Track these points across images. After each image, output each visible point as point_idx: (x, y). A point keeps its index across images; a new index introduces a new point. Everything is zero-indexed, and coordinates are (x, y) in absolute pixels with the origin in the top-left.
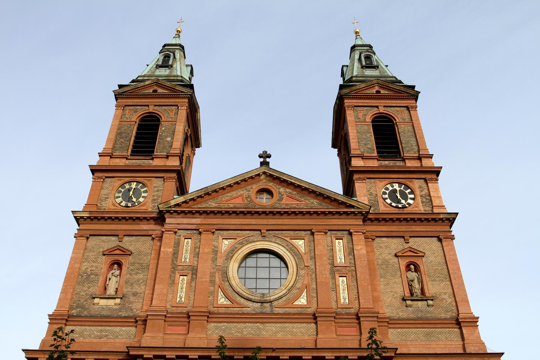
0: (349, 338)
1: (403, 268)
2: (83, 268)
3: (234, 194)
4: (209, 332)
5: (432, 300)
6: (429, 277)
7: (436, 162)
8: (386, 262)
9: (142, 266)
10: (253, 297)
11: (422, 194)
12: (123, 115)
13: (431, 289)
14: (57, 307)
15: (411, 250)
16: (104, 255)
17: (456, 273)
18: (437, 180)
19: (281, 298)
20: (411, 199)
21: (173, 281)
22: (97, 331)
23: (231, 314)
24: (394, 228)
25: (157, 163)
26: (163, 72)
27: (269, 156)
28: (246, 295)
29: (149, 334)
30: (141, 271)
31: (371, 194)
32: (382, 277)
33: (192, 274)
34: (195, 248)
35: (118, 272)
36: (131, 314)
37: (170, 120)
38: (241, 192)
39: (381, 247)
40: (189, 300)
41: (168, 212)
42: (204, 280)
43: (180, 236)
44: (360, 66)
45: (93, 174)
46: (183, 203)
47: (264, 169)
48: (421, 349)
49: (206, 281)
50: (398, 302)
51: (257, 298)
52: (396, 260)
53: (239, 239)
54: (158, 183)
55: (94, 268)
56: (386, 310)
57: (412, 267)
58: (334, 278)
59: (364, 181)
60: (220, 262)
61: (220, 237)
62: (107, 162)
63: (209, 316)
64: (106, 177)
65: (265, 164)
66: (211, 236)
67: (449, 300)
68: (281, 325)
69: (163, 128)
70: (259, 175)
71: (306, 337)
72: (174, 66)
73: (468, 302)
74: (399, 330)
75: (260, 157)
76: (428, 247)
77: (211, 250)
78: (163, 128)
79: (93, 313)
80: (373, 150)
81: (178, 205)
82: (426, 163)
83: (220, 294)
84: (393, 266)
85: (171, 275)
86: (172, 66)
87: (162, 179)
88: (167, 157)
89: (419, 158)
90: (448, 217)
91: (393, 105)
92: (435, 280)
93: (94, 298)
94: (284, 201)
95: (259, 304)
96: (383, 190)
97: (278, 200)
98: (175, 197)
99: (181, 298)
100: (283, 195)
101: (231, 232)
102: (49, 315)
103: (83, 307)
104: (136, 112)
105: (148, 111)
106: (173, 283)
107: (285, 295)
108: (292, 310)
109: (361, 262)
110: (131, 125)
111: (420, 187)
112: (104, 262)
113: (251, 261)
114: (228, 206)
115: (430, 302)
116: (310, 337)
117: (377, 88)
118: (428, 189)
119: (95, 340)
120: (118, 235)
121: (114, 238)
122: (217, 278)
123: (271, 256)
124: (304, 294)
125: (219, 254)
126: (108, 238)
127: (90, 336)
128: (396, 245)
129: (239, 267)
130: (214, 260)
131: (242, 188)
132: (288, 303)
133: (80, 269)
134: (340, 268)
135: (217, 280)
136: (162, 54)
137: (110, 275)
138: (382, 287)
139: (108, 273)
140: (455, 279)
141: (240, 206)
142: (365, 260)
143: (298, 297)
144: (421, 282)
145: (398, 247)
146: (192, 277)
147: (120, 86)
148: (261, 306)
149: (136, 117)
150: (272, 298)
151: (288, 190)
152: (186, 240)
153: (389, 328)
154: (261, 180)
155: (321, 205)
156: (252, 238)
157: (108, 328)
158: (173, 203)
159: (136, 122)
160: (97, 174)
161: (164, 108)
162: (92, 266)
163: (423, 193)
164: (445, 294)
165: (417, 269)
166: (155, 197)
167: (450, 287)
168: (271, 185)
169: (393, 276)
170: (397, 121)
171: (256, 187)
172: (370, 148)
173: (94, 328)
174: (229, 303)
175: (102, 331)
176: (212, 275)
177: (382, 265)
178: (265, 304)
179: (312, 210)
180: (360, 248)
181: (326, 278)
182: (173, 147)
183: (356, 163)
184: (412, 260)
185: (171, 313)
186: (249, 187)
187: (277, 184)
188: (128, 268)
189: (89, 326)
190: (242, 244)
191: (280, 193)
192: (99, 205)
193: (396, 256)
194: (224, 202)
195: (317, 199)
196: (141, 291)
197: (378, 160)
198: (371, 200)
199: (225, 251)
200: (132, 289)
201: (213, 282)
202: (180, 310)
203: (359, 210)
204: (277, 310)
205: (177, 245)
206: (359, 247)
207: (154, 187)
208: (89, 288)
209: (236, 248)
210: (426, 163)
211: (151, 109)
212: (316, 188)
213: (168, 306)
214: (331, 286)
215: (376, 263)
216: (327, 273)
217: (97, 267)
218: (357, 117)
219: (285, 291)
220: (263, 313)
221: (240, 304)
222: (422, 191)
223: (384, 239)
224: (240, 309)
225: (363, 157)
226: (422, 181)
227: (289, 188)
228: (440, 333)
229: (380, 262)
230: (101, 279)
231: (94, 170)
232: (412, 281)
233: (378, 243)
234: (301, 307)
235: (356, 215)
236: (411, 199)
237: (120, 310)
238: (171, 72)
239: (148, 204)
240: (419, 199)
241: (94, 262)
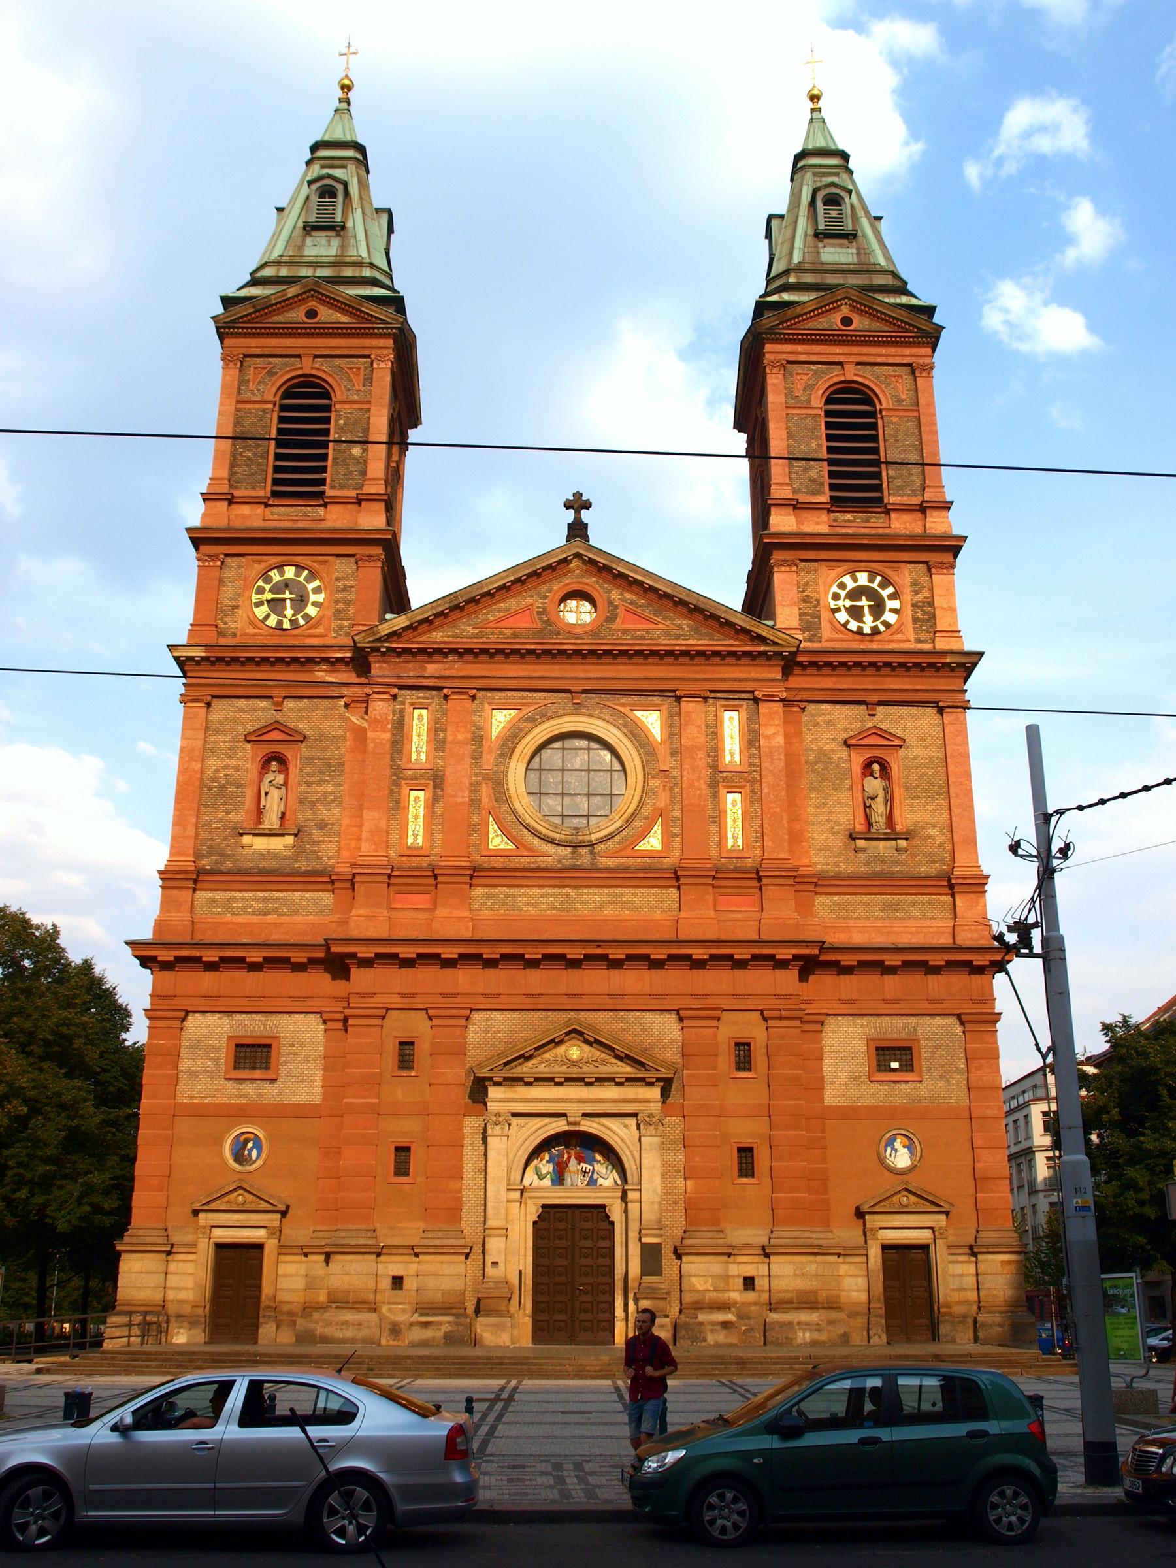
0: (739, 916)
1: (857, 769)
2: (210, 771)
3: (512, 604)
4: (475, 906)
5: (907, 839)
6: (908, 789)
7: (956, 522)
8: (824, 758)
9: (329, 765)
10: (556, 836)
11: (916, 599)
12: (242, 383)
13: (906, 817)
14: (171, 854)
15: (878, 732)
16: (249, 742)
17: (961, 784)
18: (953, 567)
19: (610, 836)
20: (893, 611)
21: (398, 802)
22: (257, 901)
23: (515, 870)
24: (847, 682)
25: (335, 518)
26: (322, 248)
27: (587, 505)
28: (544, 831)
29: (361, 912)
30: (329, 776)
31: (806, 599)
32: (812, 788)
33: (435, 787)
34: (436, 729)
35: (280, 779)
36: (320, 867)
37: (356, 398)
38: (529, 601)
39: (817, 724)
40: (432, 841)
41: (377, 650)
42: (459, 800)
43: (403, 703)
44: (810, 231)
45: (197, 548)
46: (405, 629)
47: (578, 546)
48: (873, 935)
49: (462, 803)
50: (839, 843)
51: (563, 837)
52: (844, 753)
53: (526, 710)
54: (343, 568)
55: (231, 771)
56: (815, 859)
57: (876, 767)
58: (716, 796)
59: (794, 569)
60: (489, 761)
61: (486, 706)
62: (223, 516)
63: (474, 874)
64: (227, 555)
65: (577, 530)
66: (468, 704)
67: (940, 839)
68: (611, 890)
69: (341, 422)
70: (565, 561)
71: (658, 915)
72: (349, 224)
73: (976, 844)
74: (836, 898)
75: (568, 505)
76: (913, 726)
77: (470, 736)
78: (341, 422)
79: (243, 864)
80: (822, 484)
82: (935, 524)
83: (493, 827)
84: (837, 766)
85: (392, 790)
86: (343, 227)
87: (352, 560)
88: (359, 502)
89: (923, 509)
90: (963, 660)
91: (879, 360)
92: (917, 797)
93: (241, 835)
94: (618, 624)
95: (569, 850)
96: (835, 589)
97: (607, 620)
98: (388, 616)
99: (415, 836)
100: (616, 607)
101: (509, 693)
102: (160, 872)
103: (221, 853)
104: (271, 373)
105: (300, 372)
106: (398, 807)
107: (619, 831)
108: (632, 862)
109: (772, 763)
110: (264, 410)
111: (915, 583)
112: (248, 758)
113: (551, 756)
114: (501, 633)
115: (902, 843)
116: (665, 916)
117: (845, 310)
118: (931, 589)
119: (256, 919)
120: (271, 697)
121: (263, 703)
122: (484, 795)
123: (594, 745)
124: (657, 829)
125: (486, 745)
126: (251, 702)
127: (244, 909)
128: (848, 719)
129: (527, 769)
130: (477, 756)
131: (529, 589)
132: (625, 849)
133: (202, 772)
134: (730, 775)
135: (485, 800)
136: (314, 187)
137: (265, 786)
138: (811, 810)
139: (261, 781)
140: (957, 796)
142: (780, 759)
143: (644, 834)
144: (889, 800)
145: (851, 723)
146: (435, 794)
147: (227, 301)
148: (573, 853)
149: (274, 389)
150: (594, 837)
151: (628, 596)
152: (417, 712)
153: (816, 893)
154: (569, 572)
156: (553, 707)
157: (277, 894)
158: (384, 629)
159: (275, 405)
160: (203, 548)
161: (338, 362)
162: (227, 767)
163: (920, 597)
164: (934, 825)
166: (341, 606)
167: (945, 811)
168: (591, 583)
169: (836, 787)
170: (884, 406)
171: (559, 586)
172: (814, 481)
173: (251, 894)
174: (511, 846)
175: (265, 900)
176: (474, 789)
177: (816, 763)
178: (580, 850)
179: (677, 648)
180: (774, 734)
181: (700, 796)
182: (369, 475)
183: (782, 522)
184: (877, 753)
185: (399, 869)
186: (545, 588)
187: (606, 581)
188: (301, 770)
189: (240, 890)
190: (533, 721)
191: (610, 603)
192: (220, 623)
193: (846, 744)
194: (492, 625)
195: (690, 619)
196: (332, 819)
197: (829, 511)
198: (805, 614)
199: (497, 737)
200: (314, 813)
201: (475, 804)
202: (415, 862)
203: (776, 649)
204: (604, 862)
205: (400, 728)
206: (770, 731)
207: (337, 579)
208: (228, 813)
209: (521, 730)
210: (935, 524)
211: (307, 366)
212: (688, 595)
213: (393, 855)
214: (710, 812)
215: (803, 759)
216: (704, 787)
217: (236, 769)
218: (789, 393)
219: (618, 824)
220: (576, 868)
221: (533, 851)
222: (917, 593)
223: (824, 706)
224: (533, 860)
225: (796, 506)
226: (922, 568)
227: (630, 591)
228: (913, 904)
229: (812, 756)
230: (250, 794)
231: (199, 539)
232: (872, 799)
233: (813, 716)
234: (651, 855)
235: (769, 658)
236: (893, 611)
237: (296, 857)
238: (343, 247)
239: (325, 622)
240: (909, 613)
241: (230, 757)
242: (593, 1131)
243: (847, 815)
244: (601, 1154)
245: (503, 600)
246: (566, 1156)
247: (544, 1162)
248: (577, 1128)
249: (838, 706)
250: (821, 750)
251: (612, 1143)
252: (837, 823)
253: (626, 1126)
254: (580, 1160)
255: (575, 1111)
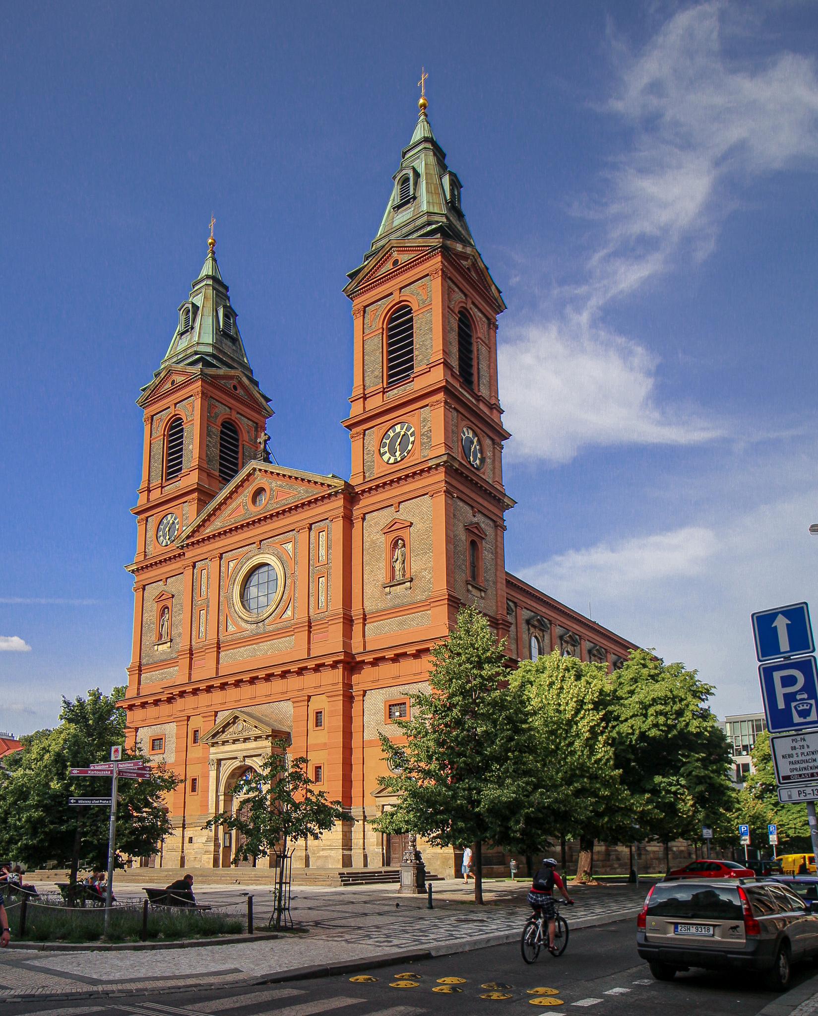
3: (234, 505)
5: (410, 582)
41: (182, 546)
81: (188, 537)
128: (383, 518)
141: (240, 519)
155: (307, 492)
158: (184, 536)
164: (425, 569)
165: (404, 546)
191: (271, 490)
243: (382, 575)
245: (231, 504)
249: (380, 512)
250: (372, 540)
252: (378, 581)
255: (240, 755)
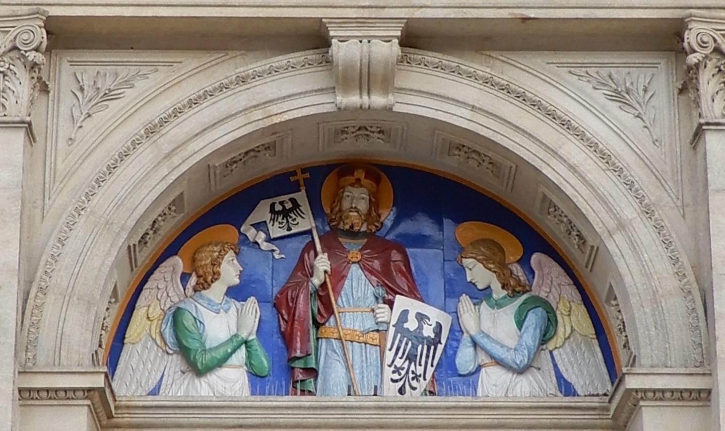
242: (460, 118)
244: (494, 258)
246: (322, 263)
247: (217, 291)
248: (378, 100)
251: (554, 172)
253: (620, 96)
254: (394, 281)
